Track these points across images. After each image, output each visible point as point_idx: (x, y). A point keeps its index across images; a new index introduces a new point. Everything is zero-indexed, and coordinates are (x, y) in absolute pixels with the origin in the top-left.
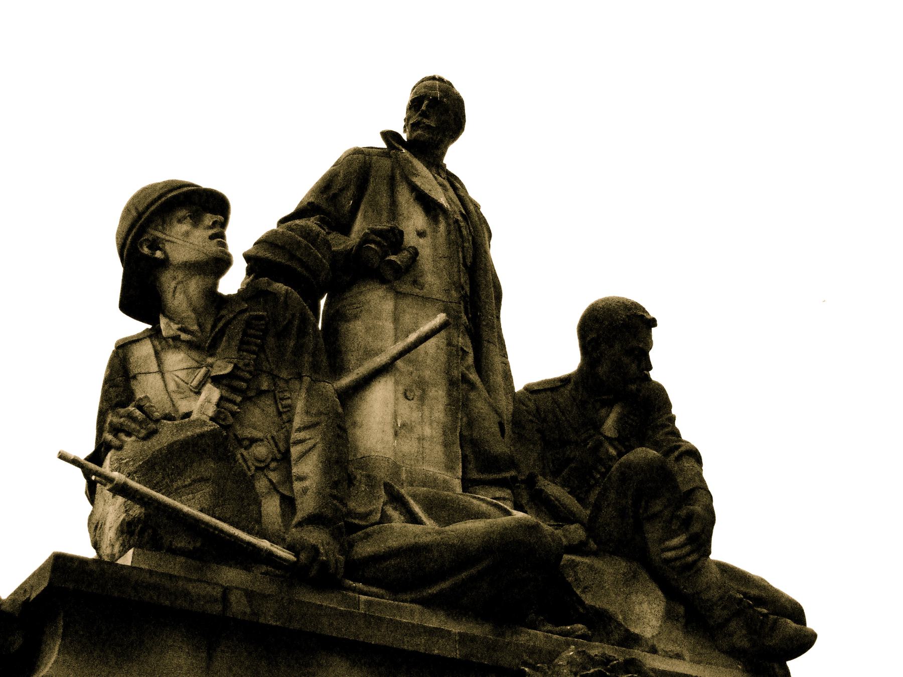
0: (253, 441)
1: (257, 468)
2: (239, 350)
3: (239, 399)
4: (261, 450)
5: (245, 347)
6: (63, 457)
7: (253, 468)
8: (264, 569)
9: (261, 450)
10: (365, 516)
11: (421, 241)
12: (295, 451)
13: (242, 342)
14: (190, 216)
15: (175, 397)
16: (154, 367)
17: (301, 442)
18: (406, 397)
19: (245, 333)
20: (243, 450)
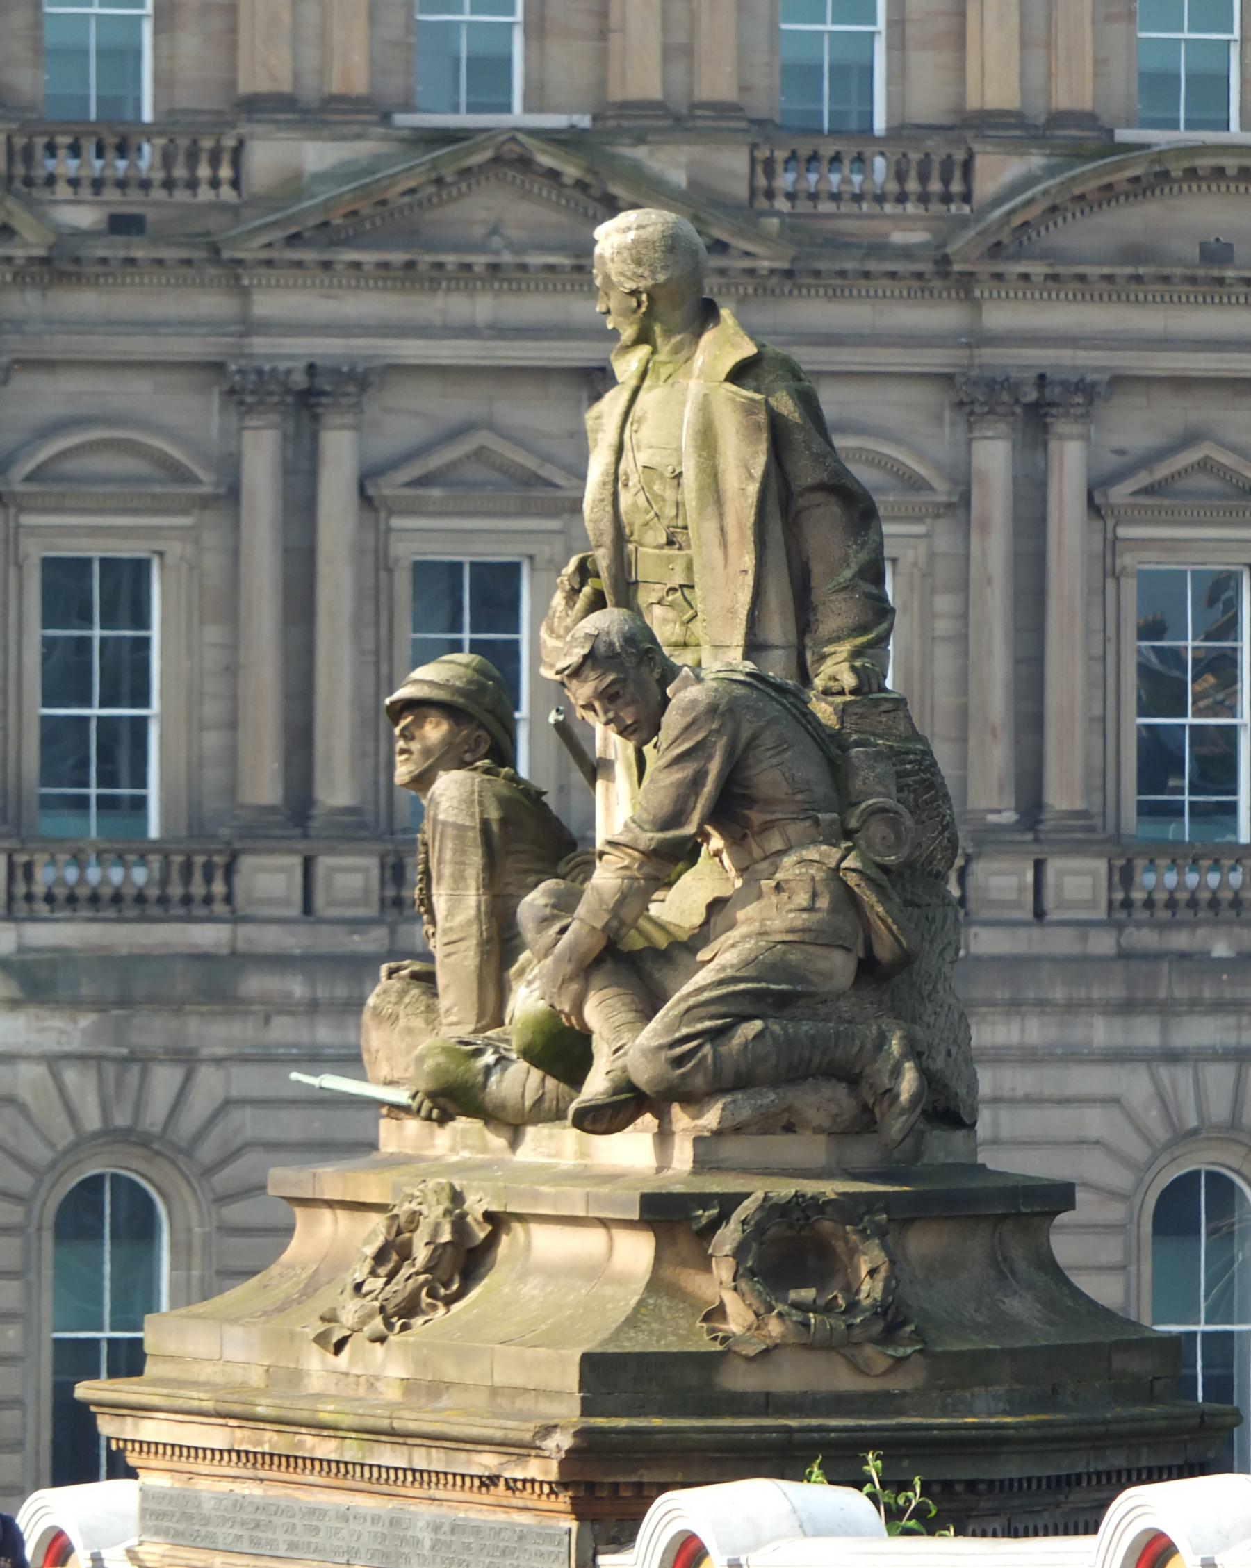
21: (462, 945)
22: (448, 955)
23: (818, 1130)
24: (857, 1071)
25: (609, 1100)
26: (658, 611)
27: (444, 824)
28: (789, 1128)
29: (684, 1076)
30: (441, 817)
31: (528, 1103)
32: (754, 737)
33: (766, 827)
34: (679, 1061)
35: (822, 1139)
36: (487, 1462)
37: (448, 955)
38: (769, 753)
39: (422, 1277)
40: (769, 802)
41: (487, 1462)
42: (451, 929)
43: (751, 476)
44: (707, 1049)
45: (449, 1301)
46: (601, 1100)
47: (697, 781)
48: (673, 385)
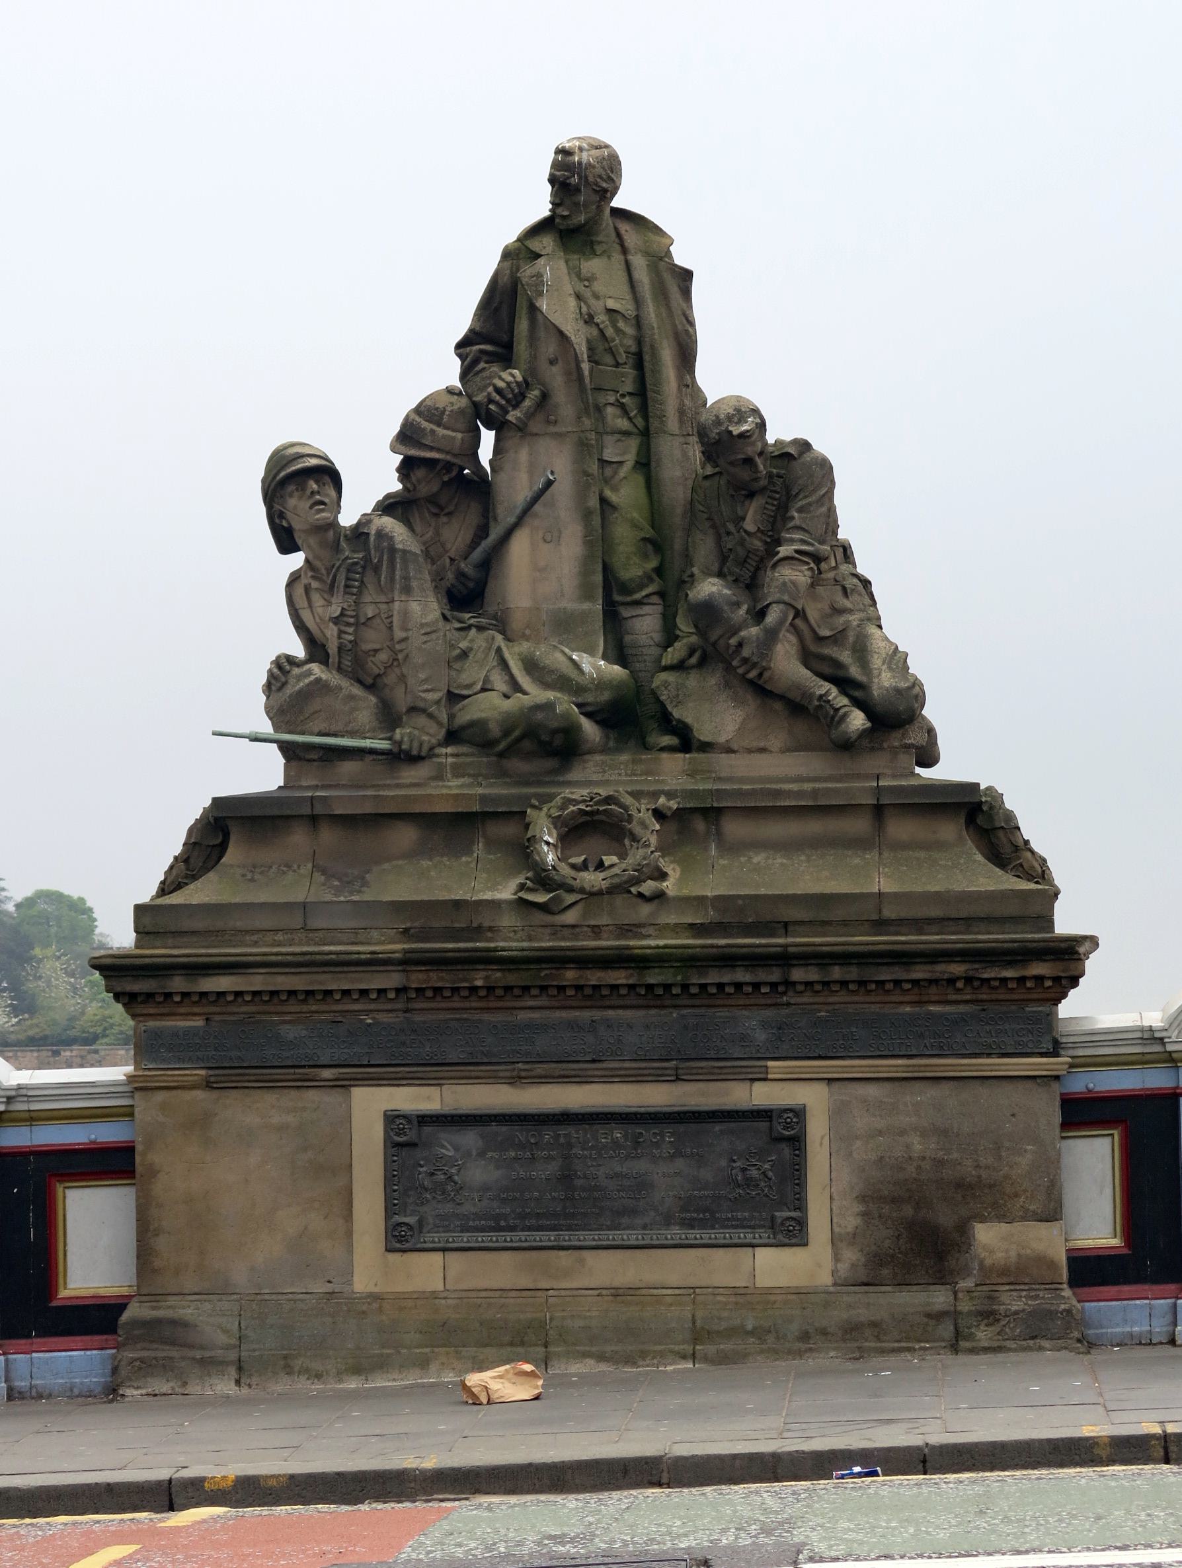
0: (376, 651)
1: (385, 668)
2: (346, 593)
3: (351, 630)
4: (383, 656)
5: (348, 590)
6: (214, 734)
7: (382, 668)
8: (372, 757)
9: (383, 656)
10: (468, 686)
11: (554, 369)
12: (400, 656)
13: (347, 586)
14: (297, 489)
15: (322, 627)
16: (306, 604)
17: (401, 651)
18: (545, 541)
19: (348, 579)
20: (373, 659)
21: (434, 636)
22: (425, 642)
26: (610, 410)
36: (957, 969)
37: (425, 642)
41: (957, 969)
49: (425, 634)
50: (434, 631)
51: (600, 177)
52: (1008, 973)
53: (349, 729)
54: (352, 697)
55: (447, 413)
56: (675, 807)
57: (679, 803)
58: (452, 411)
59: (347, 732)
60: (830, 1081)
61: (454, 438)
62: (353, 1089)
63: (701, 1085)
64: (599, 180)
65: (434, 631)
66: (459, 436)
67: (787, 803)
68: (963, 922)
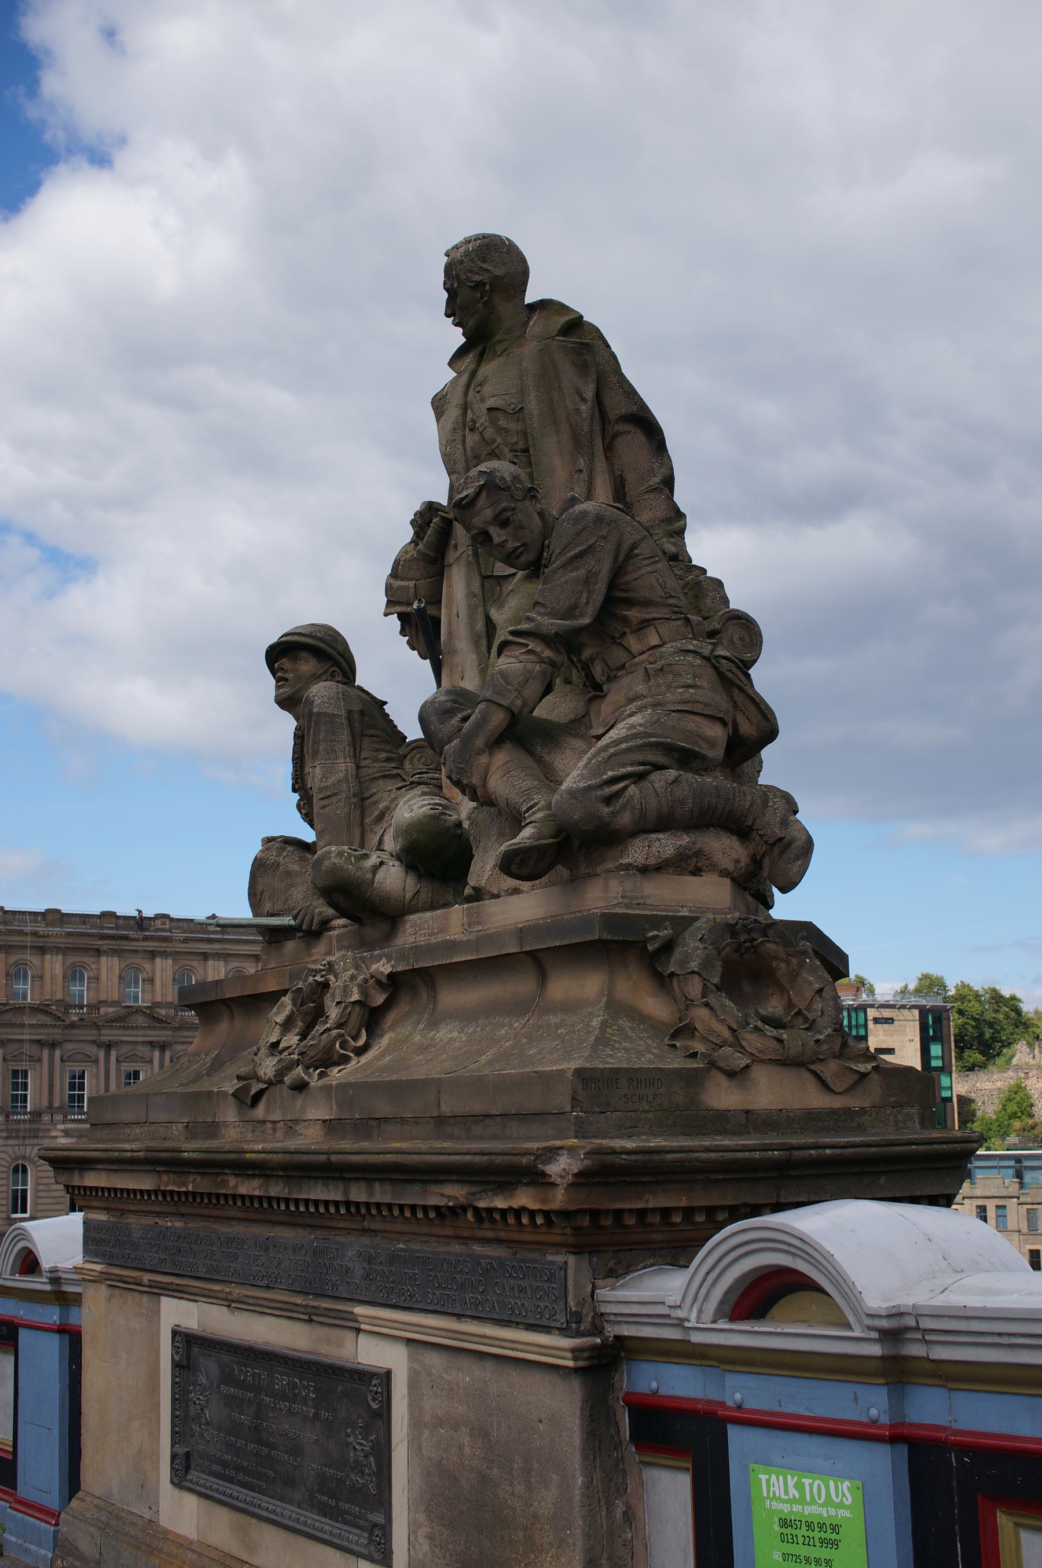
21: (334, 799)
22: (324, 807)
23: (724, 873)
24: (749, 823)
25: (535, 843)
27: (319, 714)
28: (696, 872)
29: (614, 814)
30: (315, 710)
31: (409, 895)
32: (634, 546)
33: (645, 624)
34: (608, 800)
35: (727, 881)
36: (454, 1193)
37: (324, 807)
38: (646, 562)
39: (335, 1032)
40: (646, 604)
41: (454, 1193)
42: (326, 788)
43: (584, 400)
44: (633, 789)
45: (360, 1051)
46: (529, 843)
47: (588, 580)
48: (508, 355)
49: (321, 799)
50: (335, 794)
51: (471, 271)
52: (500, 1203)
53: (286, 907)
54: (288, 874)
55: (402, 562)
56: (389, 970)
57: (393, 966)
58: (405, 560)
59: (286, 910)
60: (409, 1341)
61: (407, 588)
62: (163, 1299)
63: (327, 1330)
64: (470, 275)
65: (335, 794)
66: (412, 584)
67: (459, 959)
68: (499, 1119)
